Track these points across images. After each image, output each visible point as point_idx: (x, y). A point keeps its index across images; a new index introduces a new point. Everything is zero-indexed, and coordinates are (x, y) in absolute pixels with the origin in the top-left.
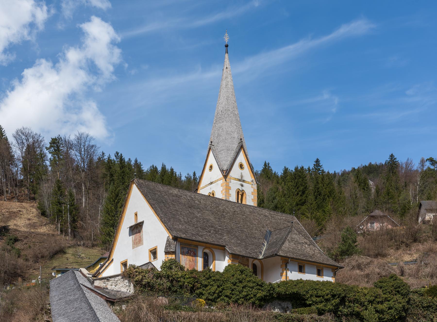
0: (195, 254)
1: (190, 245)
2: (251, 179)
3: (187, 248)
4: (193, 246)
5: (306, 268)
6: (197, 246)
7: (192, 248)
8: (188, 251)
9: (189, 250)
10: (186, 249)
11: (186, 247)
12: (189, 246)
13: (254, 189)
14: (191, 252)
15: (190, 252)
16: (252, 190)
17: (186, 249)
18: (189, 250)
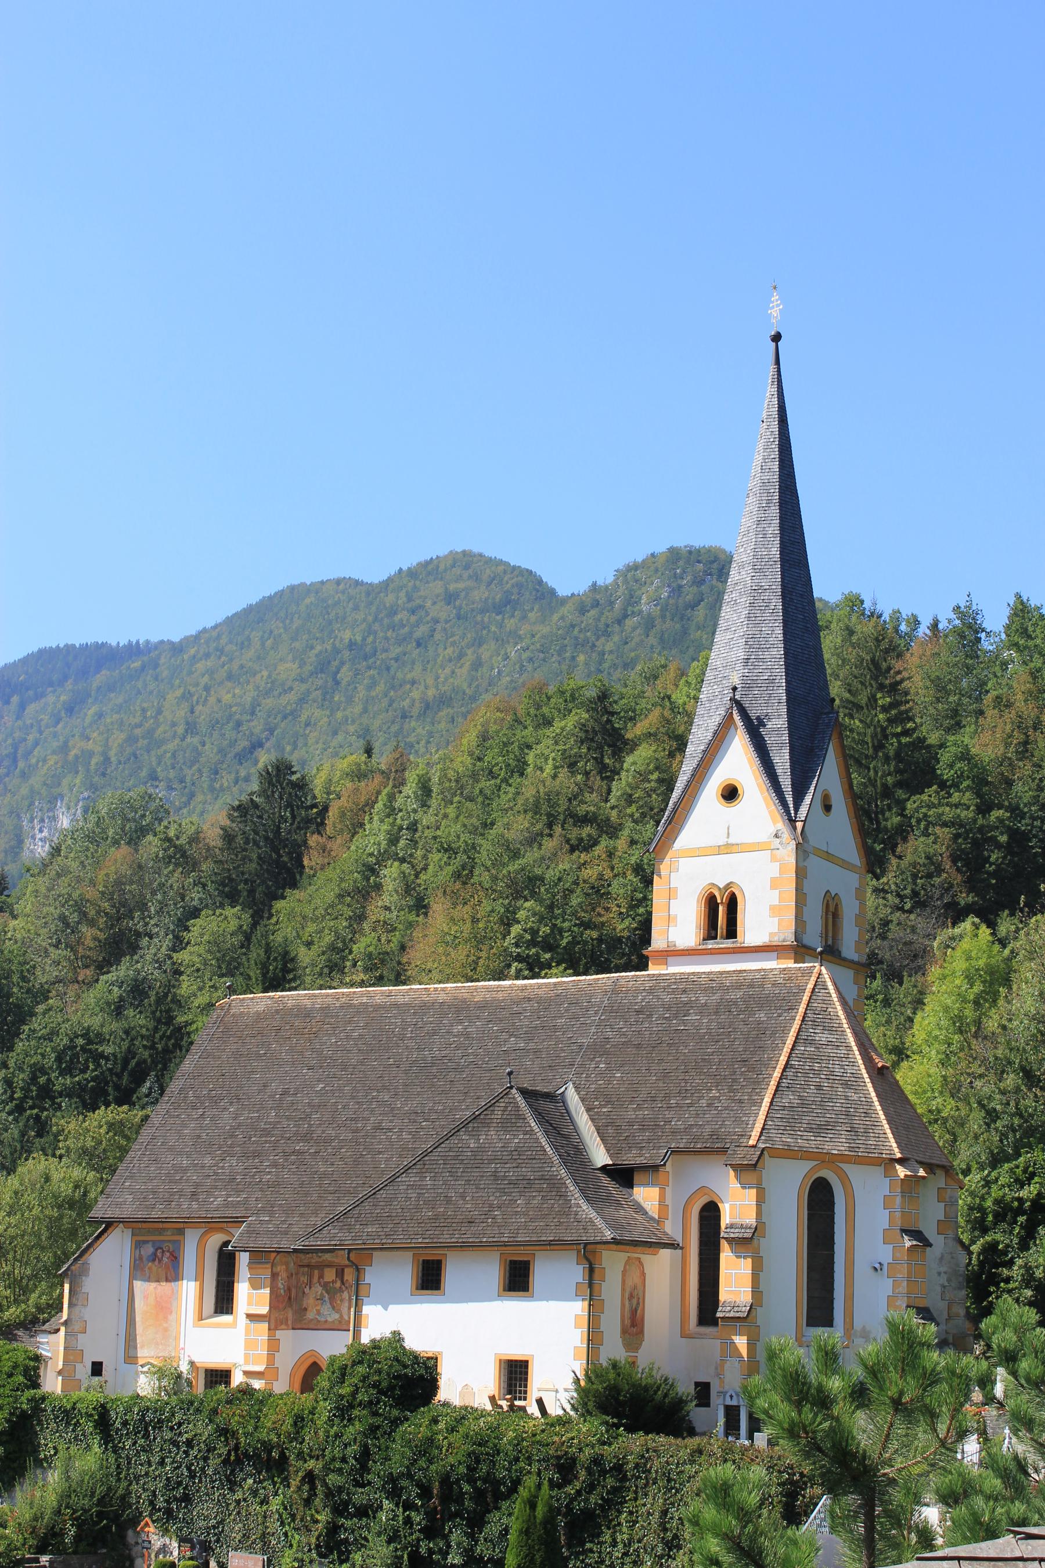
0: (176, 1258)
1: (161, 1231)
2: (772, 830)
3: (154, 1242)
4: (169, 1233)
5: (451, 1275)
6: (181, 1232)
7: (169, 1241)
8: (155, 1254)
9: (157, 1250)
10: (150, 1245)
11: (147, 1242)
12: (160, 1234)
13: (782, 871)
14: (163, 1252)
15: (159, 1253)
16: (774, 870)
17: (150, 1245)
18: (157, 1250)
